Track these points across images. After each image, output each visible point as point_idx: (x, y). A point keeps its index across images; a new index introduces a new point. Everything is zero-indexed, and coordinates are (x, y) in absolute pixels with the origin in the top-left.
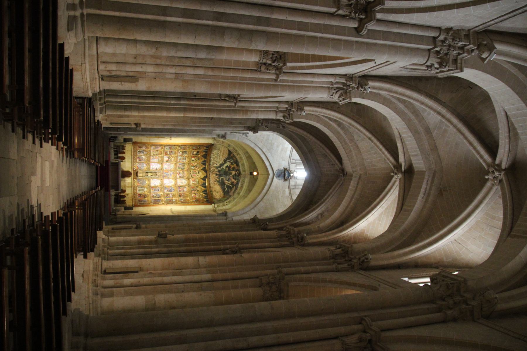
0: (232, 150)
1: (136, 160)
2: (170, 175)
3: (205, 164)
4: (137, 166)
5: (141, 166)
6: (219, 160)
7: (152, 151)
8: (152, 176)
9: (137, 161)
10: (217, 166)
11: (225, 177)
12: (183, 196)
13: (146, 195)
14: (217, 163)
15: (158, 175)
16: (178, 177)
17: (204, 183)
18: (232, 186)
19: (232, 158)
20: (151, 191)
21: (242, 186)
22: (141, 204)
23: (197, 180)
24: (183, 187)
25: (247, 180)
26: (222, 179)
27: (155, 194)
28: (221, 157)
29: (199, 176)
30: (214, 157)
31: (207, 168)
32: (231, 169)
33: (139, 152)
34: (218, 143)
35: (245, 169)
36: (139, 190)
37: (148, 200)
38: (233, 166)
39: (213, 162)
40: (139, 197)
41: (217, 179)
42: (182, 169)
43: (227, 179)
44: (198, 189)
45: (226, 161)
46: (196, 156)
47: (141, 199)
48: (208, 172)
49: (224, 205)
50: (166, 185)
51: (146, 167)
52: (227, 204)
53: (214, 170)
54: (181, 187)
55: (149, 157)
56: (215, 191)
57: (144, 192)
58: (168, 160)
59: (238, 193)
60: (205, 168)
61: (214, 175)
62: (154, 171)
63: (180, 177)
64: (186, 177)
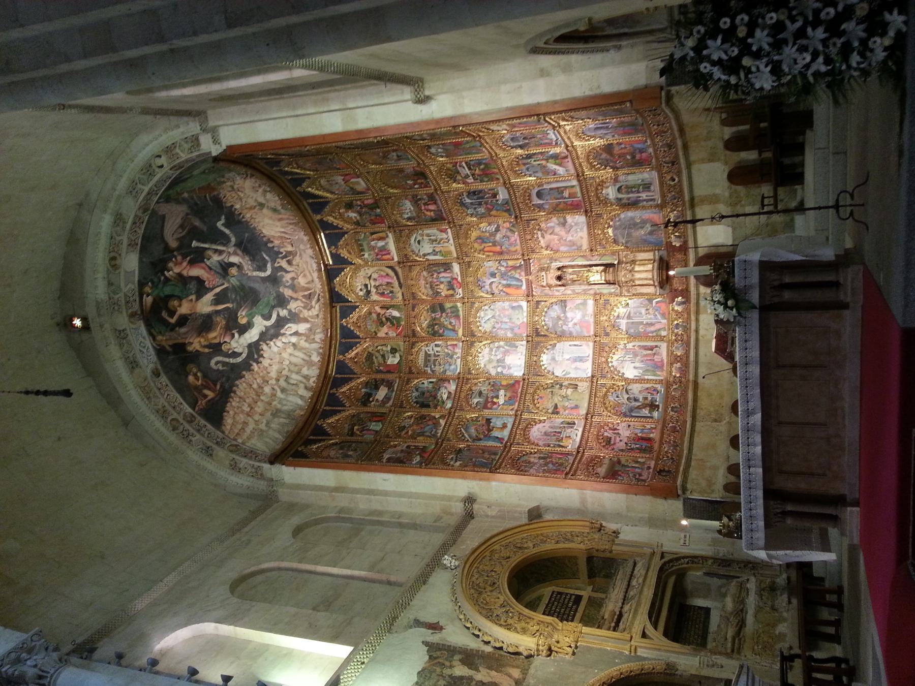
0: (192, 431)
1: (670, 353)
2: (493, 275)
3: (347, 333)
4: (663, 315)
9: (664, 346)
10: (293, 327)
11: (249, 278)
12: (408, 177)
14: (294, 339)
15: (554, 273)
16: (456, 268)
17: (336, 247)
18: (194, 244)
19: (210, 378)
20: (578, 189)
21: (113, 262)
22: (621, 112)
23: (366, 256)
25: (97, 289)
26: (262, 268)
27: (555, 174)
28: (273, 374)
29: (362, 273)
32: (221, 321)
33: (653, 406)
35: (121, 346)
36: (647, 187)
38: (212, 335)
39: (314, 341)
40: (641, 151)
41: (284, 264)
42: (442, 309)
43: (233, 271)
44: (352, 215)
45: (250, 356)
46: (379, 376)
47: (627, 139)
49: (169, 150)
52: (159, 162)
53: (308, 307)
55: (600, 370)
57: (616, 180)
58: (506, 353)
59: (124, 223)
61: (302, 281)
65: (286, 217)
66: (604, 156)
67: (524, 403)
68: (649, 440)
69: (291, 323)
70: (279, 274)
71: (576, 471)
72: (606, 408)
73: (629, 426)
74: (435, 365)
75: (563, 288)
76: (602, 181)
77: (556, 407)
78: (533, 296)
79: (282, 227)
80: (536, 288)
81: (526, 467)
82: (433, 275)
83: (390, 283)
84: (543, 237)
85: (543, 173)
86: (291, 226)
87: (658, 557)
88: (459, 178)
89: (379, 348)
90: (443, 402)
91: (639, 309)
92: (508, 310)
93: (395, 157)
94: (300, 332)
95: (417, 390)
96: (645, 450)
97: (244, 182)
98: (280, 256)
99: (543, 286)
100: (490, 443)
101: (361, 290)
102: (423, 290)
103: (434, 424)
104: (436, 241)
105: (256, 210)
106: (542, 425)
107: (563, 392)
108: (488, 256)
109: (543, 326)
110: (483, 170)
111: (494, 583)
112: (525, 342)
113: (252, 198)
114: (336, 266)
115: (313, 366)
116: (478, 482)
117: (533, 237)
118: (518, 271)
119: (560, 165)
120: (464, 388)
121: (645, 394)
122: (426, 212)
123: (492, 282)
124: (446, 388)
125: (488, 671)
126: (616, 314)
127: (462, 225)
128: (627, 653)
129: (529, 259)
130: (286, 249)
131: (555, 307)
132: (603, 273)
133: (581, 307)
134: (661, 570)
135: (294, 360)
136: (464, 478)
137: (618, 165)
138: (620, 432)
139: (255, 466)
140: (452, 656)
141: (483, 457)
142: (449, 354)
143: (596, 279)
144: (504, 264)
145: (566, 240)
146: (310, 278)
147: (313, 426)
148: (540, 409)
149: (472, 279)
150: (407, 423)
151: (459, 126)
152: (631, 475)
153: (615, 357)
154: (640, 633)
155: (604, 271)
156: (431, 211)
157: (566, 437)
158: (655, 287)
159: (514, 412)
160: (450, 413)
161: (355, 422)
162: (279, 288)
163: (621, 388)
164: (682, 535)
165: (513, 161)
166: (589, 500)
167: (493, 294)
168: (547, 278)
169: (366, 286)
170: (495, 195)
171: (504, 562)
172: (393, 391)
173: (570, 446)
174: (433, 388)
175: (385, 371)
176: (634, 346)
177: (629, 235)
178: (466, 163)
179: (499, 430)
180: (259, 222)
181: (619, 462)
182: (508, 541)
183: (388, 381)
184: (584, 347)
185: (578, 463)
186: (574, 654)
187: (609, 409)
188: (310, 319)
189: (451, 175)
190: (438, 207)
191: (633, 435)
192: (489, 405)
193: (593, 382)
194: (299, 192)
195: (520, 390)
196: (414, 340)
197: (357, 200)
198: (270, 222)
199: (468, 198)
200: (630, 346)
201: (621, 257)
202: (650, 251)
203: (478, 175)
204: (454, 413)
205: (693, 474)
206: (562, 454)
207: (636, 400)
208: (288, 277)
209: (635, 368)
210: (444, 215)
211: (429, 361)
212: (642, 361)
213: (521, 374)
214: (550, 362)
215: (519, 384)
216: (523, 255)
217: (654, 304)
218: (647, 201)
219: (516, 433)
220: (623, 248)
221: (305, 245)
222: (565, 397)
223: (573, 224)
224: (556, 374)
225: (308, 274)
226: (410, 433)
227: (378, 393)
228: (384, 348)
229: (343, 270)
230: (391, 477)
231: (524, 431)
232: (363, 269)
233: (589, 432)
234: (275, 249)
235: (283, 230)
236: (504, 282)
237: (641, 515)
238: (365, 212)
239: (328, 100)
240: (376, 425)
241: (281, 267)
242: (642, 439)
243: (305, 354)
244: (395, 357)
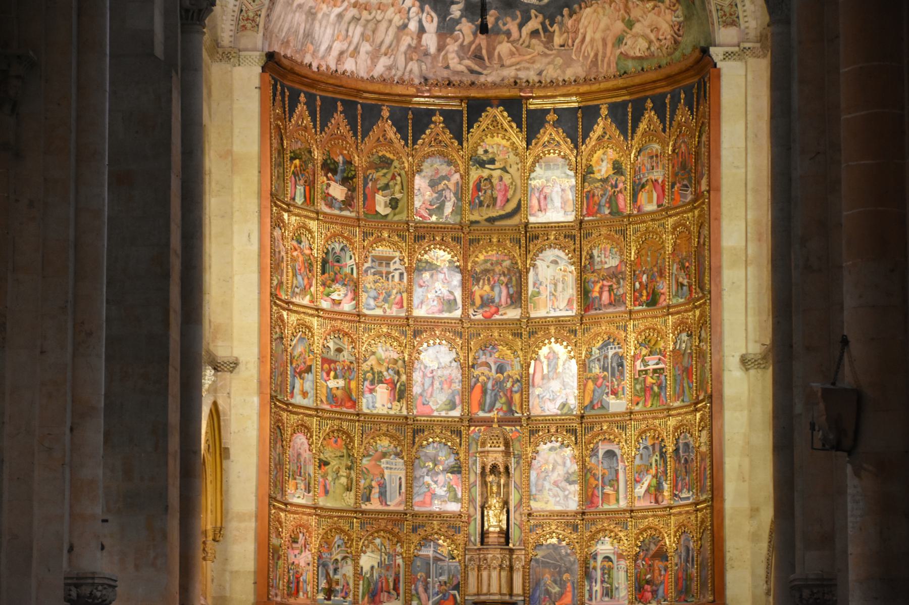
2: (501, 369)
5: (434, 587)
6: (390, 12)
7: (322, 502)
8: (506, 503)
10: (431, 26)
12: (651, 279)
13: (644, 547)
14: (413, 26)
15: (500, 459)
16: (513, 314)
17: (556, 124)
20: (613, 506)
22: (703, 585)
24: (593, 278)
27: (637, 482)
29: (512, 158)
30: (366, 47)
31: (454, 105)
34: (261, 21)
37: (682, 529)
39: (409, 59)
40: (654, 593)
41: (534, 24)
44: (603, 169)
46: (359, 181)
48: (473, 93)
50: (573, 402)
51: (445, 547)
54: (584, 292)
56: (620, 40)
57: (620, 556)
58: (392, 384)
60: (453, 121)
61: (504, 48)
62: (469, 489)
63: (517, 298)
64: (516, 253)
65: (608, 54)
66: (653, 548)
67: (329, 418)
68: (297, 592)
69: (439, 23)
70: (518, 13)
72: (326, 533)
74: (374, 274)
75: (479, 471)
76: (620, 540)
77: (326, 463)
78: (469, 426)
79: (592, 40)
80: (479, 431)
82: (505, 275)
83: (494, 204)
84: (551, 449)
85: (640, 466)
86: (592, 55)
88: (644, 351)
89: (398, 178)
90: (328, 295)
91: (446, 572)
92: (450, 387)
93: (681, 280)
94: (425, 36)
95: (342, 249)
97: (667, 22)
98: (547, 22)
99: (483, 444)
101: (486, 151)
102: (481, 258)
103: (305, 289)
104: (555, 290)
105: (622, 11)
106: (307, 446)
107: (343, 472)
108: (529, 366)
109: (427, 440)
110: (652, 388)
112: (405, 412)
113: (642, 17)
114: (524, 116)
115: (372, 60)
116: (256, 376)
117: (553, 435)
118: (505, 408)
119: (647, 491)
120: (347, 324)
121: (342, 582)
122: (599, 285)
123: (490, 367)
124: (346, 295)
126: (441, 542)
127: (575, 335)
129: (521, 426)
130: (557, 34)
131: (453, 456)
132: (498, 529)
133: (452, 494)
135: (383, 26)
136: (261, 358)
137: (639, 561)
138: (303, 554)
139: (258, 19)
142: (389, 296)
143: (491, 520)
144: (516, 388)
145: (545, 479)
146: (507, 62)
147: (297, 86)
148: (325, 442)
149: (496, 334)
150: (305, 244)
151: (711, 403)
153: (387, 543)
155: (501, 532)
156: (601, 293)
157: (297, 484)
158: (478, 594)
160: (317, 310)
161: (304, 157)
162: (496, 9)
163: (349, 551)
165: (659, 434)
167: (473, 366)
168: (496, 452)
169: (492, 161)
170: (614, 393)
172: (341, 209)
174: (346, 275)
175: (366, 192)
176: (399, 565)
177: (545, 564)
178: (663, 369)
180: (604, 8)
181: (279, 558)
183: (352, 198)
184: (398, 499)
188: (443, 53)
189: (649, 341)
190: (605, 305)
191: (300, 570)
192: (326, 366)
193: (356, 512)
194: (644, 99)
195: (344, 410)
196: (410, 238)
197: (624, 183)
198: (602, 25)
199: (616, 354)
200: (399, 561)
201: (518, 552)
202: (524, 589)
203: (645, 378)
204: (318, 316)
207: (336, 570)
208: (512, 26)
209: (372, 567)
210: (593, 312)
211: (380, 264)
212: (380, 577)
214: (380, 450)
215: (351, 407)
216: (529, 418)
217: (452, 592)
218: (590, 591)
220: (531, 555)
221: (560, 67)
222: (338, 477)
223: (567, 493)
224: (365, 461)
225: (513, 60)
226: (295, 254)
227: (337, 185)
228: (398, 188)
229: (519, 126)
230: (255, 247)
231: (302, 425)
232: (517, 159)
234: (559, 18)
235: (588, 39)
236: (490, 385)
237: (228, 586)
238: (605, 190)
239: (759, 240)
240: (301, 194)
241: (529, 18)
242: (298, 582)
243: (390, 46)
244: (386, 206)
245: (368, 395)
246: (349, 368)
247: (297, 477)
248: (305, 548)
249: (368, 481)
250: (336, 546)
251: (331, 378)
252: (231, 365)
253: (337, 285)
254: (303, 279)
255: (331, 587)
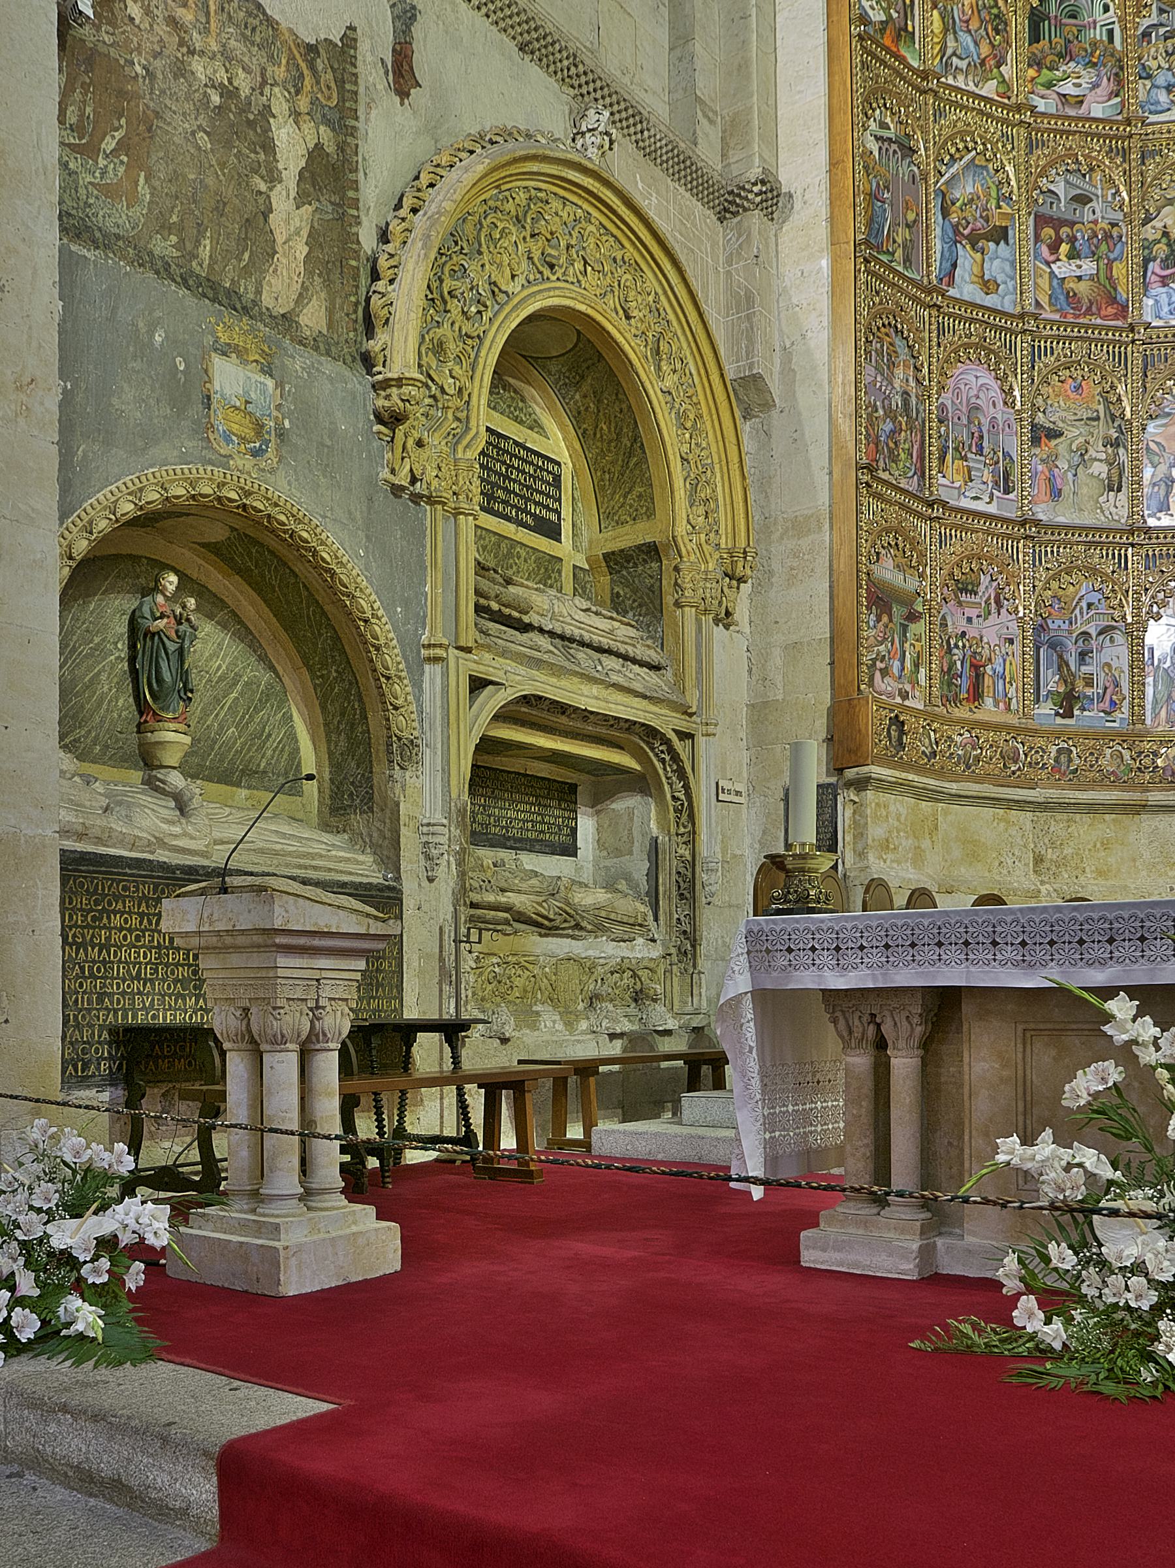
67: (1059, 338)
68: (976, 695)
71: (879, 496)
72: (1056, 577)
73: (1011, 642)
81: (880, 353)
87: (683, 724)
90: (1049, 85)
96: (950, 684)
100: (937, 246)
103: (983, 63)
106: (999, 398)
107: (1098, 451)
111: (552, 266)
124: (1095, 86)
125: (305, 233)
128: (424, 639)
134: (651, 733)
138: (993, 618)
140: (328, 122)
141: (895, 225)
148: (1045, 390)
152: (882, 648)
154: (482, 671)
159: (1028, 309)
163: (1116, 614)
164: (739, 787)
166: (805, 543)
171: (611, 301)
173: (942, 481)
174: (1094, 44)
179: (976, 270)
181: (913, 617)
182: (671, 317)
185: (902, 506)
186: (397, 490)
187: (1054, 585)
191: (986, 652)
192: (1048, 232)
195: (1099, 321)
205: (900, 805)
206: (921, 458)
213: (1148, 318)
215: (1116, 317)
219: (972, 320)
224: (1151, 428)
233: (987, 532)
242: (978, 677)
245: (1157, 290)
246: (1108, 236)
247: (969, 455)
248: (999, 605)
249: (1163, 468)
250: (1084, 604)
251: (1062, 257)
252: (756, 189)
253: (1072, 64)
254: (976, 44)
255: (1073, 689)
